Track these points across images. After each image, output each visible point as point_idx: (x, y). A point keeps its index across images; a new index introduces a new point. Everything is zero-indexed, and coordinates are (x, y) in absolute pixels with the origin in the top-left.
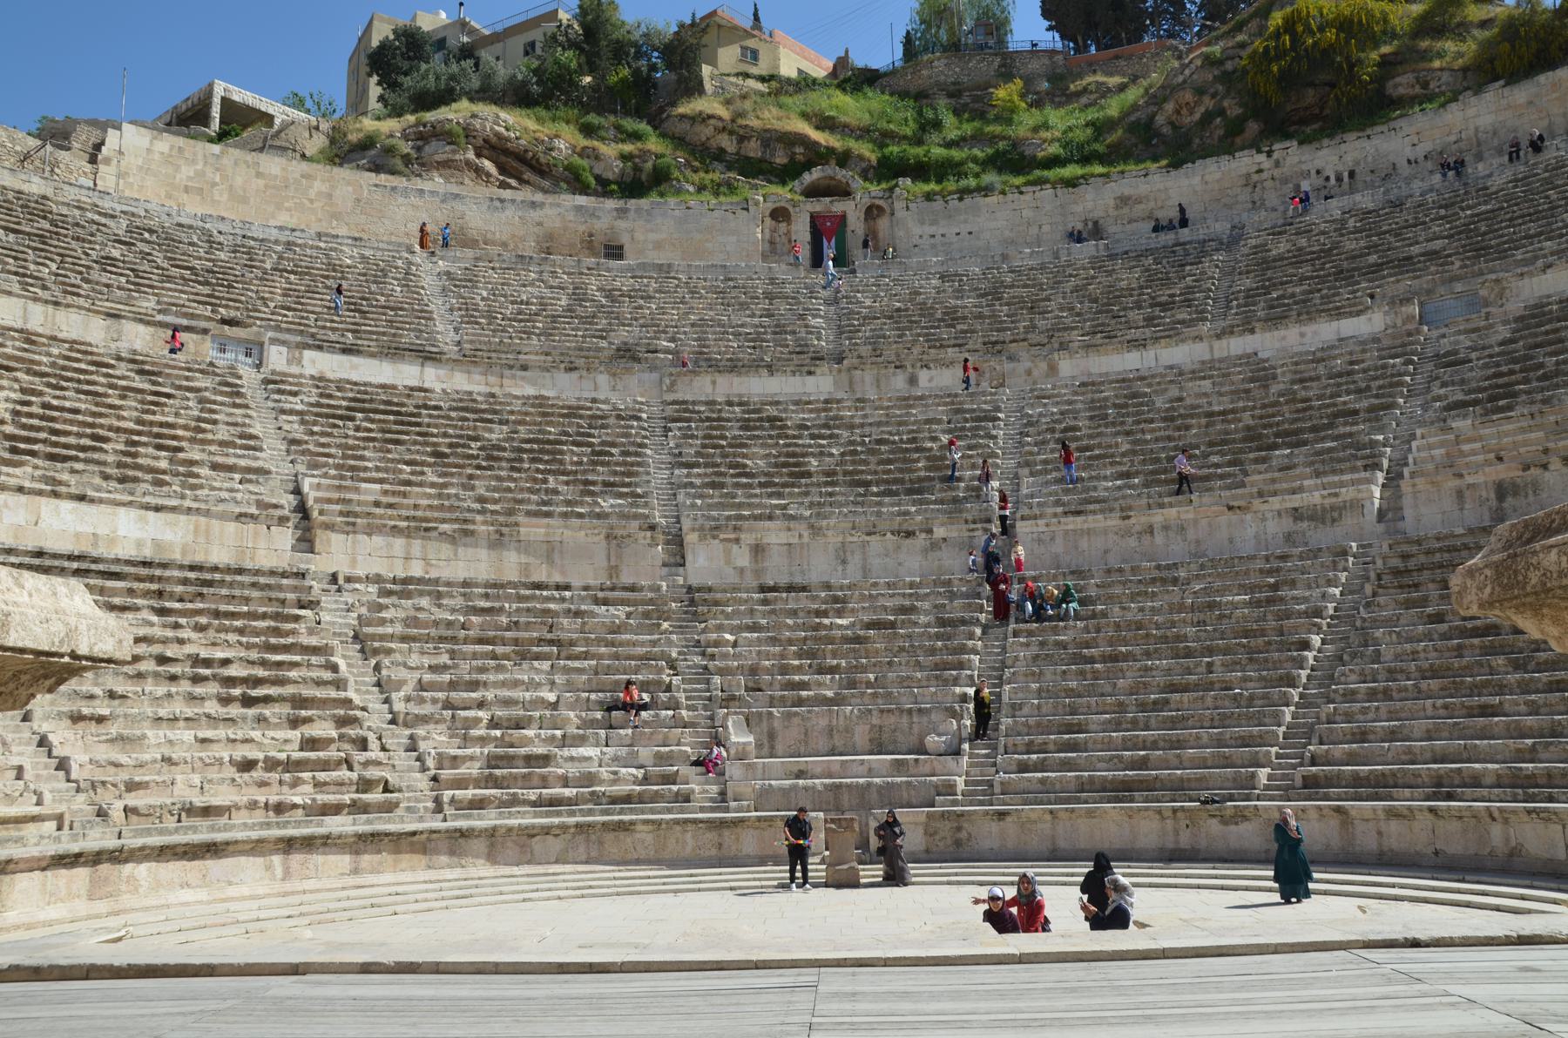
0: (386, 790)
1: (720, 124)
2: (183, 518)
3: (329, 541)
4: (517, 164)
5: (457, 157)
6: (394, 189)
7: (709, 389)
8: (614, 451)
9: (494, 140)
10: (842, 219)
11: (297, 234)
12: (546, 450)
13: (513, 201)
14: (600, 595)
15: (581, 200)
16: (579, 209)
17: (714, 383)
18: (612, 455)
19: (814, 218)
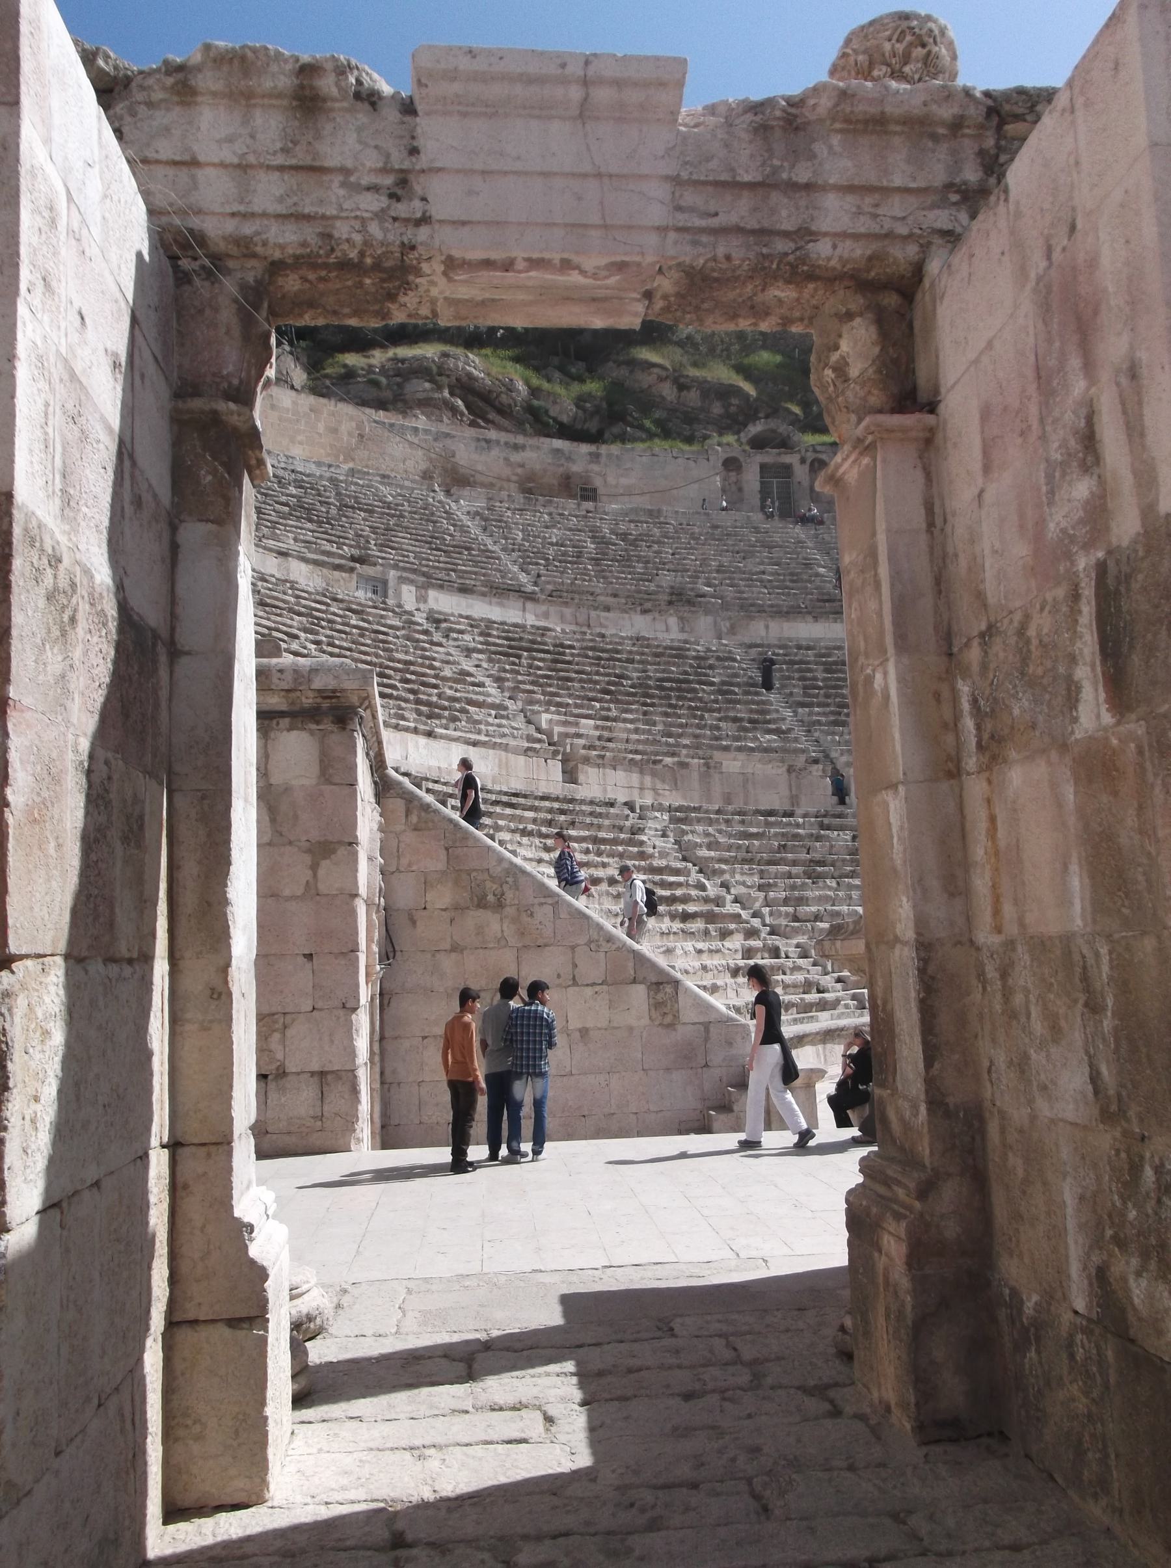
0: (819, 991)
1: (664, 374)
2: (491, 752)
3: (587, 773)
4: (482, 405)
5: (436, 395)
6: (392, 425)
7: (763, 633)
8: (736, 690)
9: (465, 379)
10: (787, 470)
11: (332, 469)
12: (683, 687)
13: (498, 442)
14: (826, 821)
15: (558, 443)
16: (558, 450)
17: (767, 627)
18: (736, 694)
19: (763, 467)
